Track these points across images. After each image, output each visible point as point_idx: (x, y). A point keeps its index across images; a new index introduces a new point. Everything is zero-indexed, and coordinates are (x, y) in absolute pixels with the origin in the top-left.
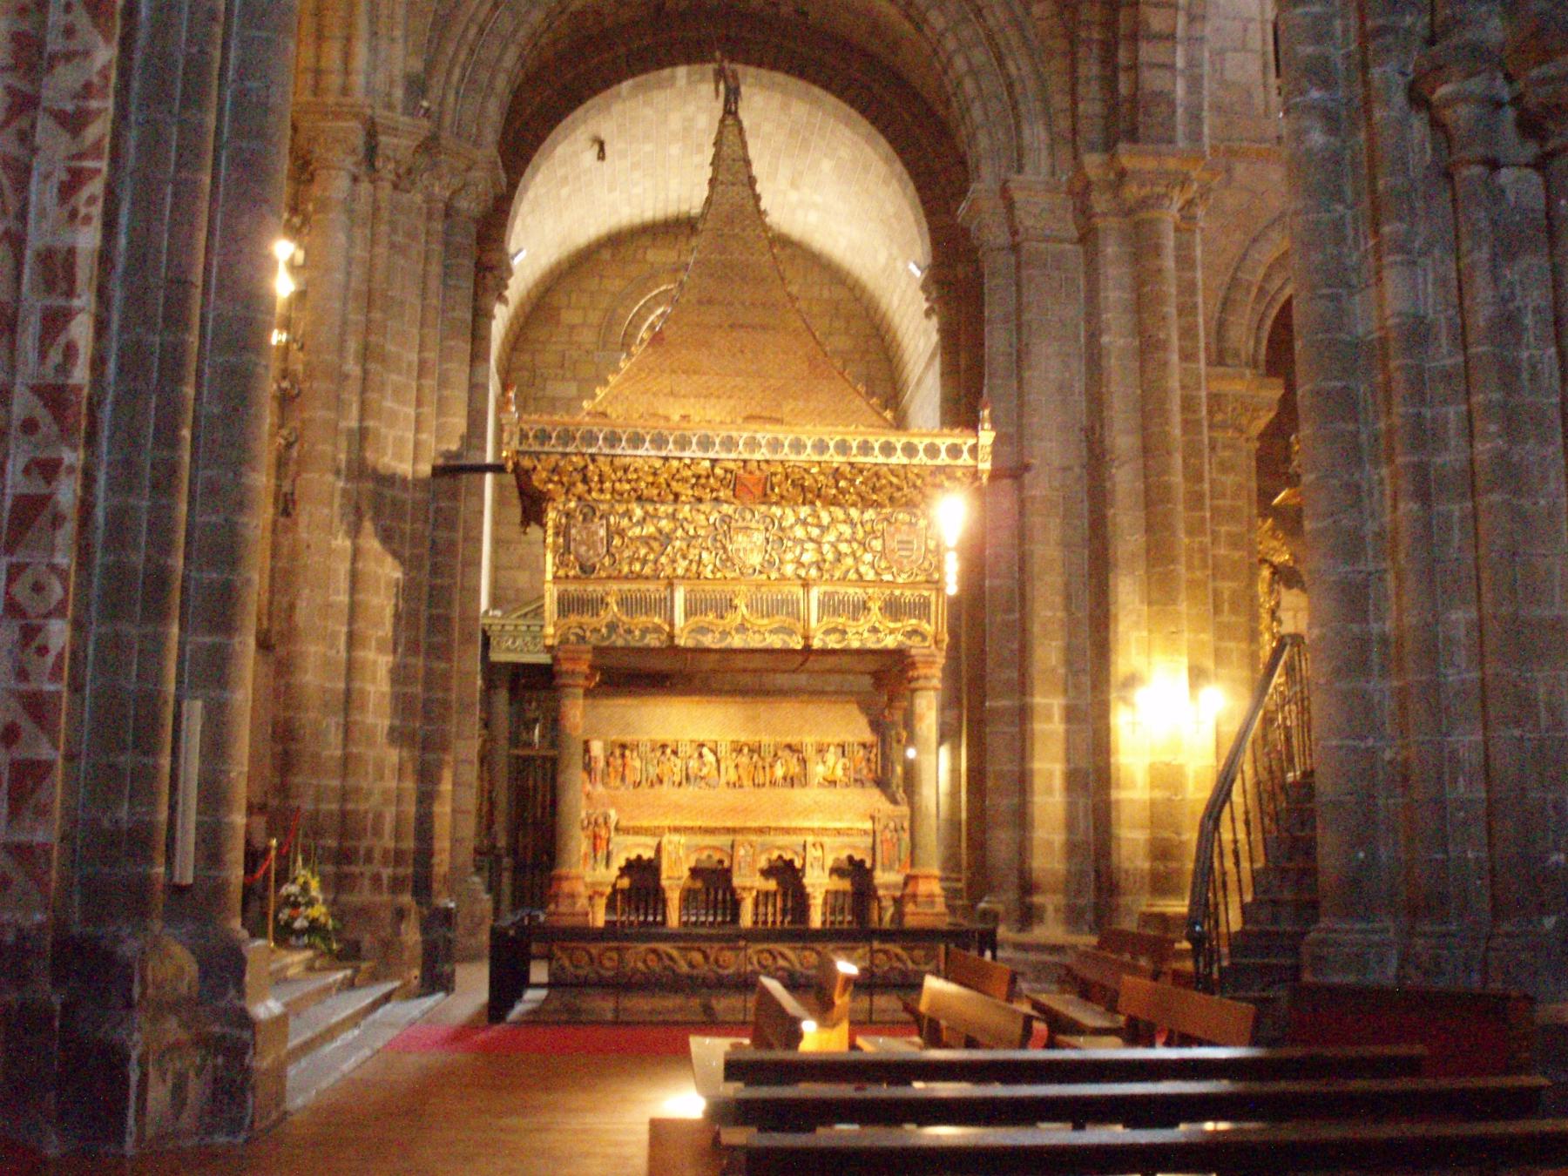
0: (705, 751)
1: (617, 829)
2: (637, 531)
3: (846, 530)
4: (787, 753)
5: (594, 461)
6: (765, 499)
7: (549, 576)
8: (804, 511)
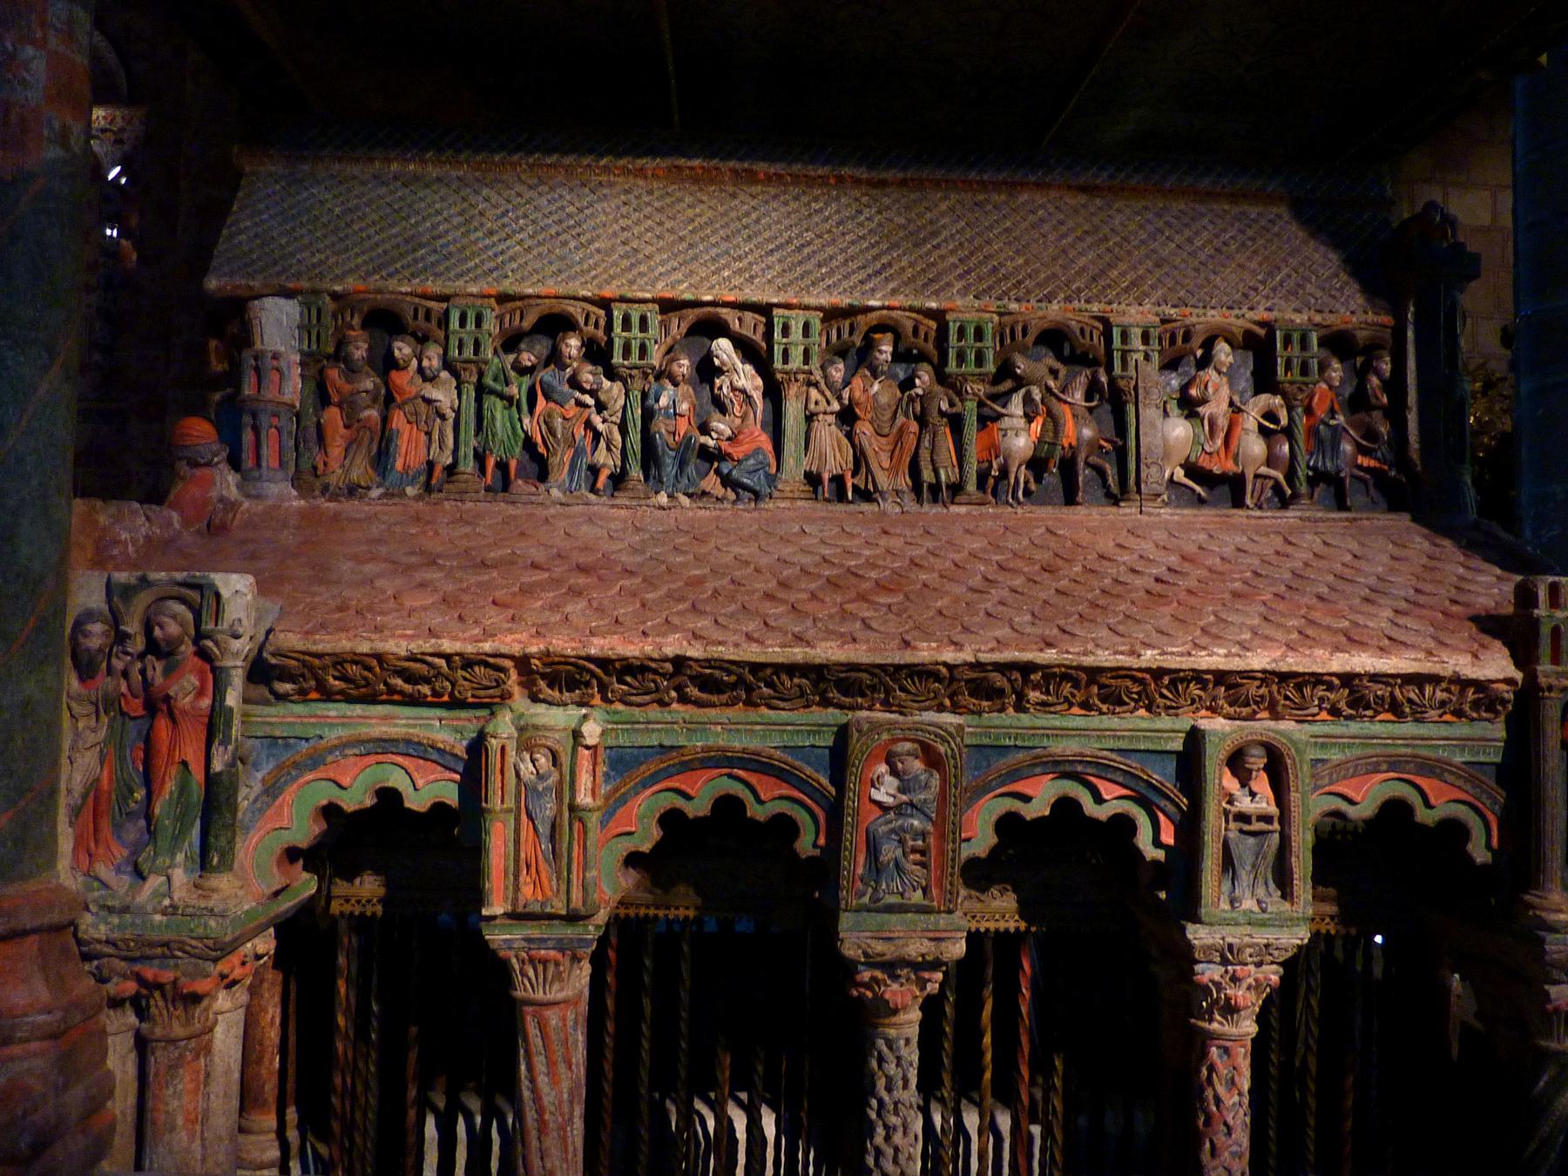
1: (261, 672)
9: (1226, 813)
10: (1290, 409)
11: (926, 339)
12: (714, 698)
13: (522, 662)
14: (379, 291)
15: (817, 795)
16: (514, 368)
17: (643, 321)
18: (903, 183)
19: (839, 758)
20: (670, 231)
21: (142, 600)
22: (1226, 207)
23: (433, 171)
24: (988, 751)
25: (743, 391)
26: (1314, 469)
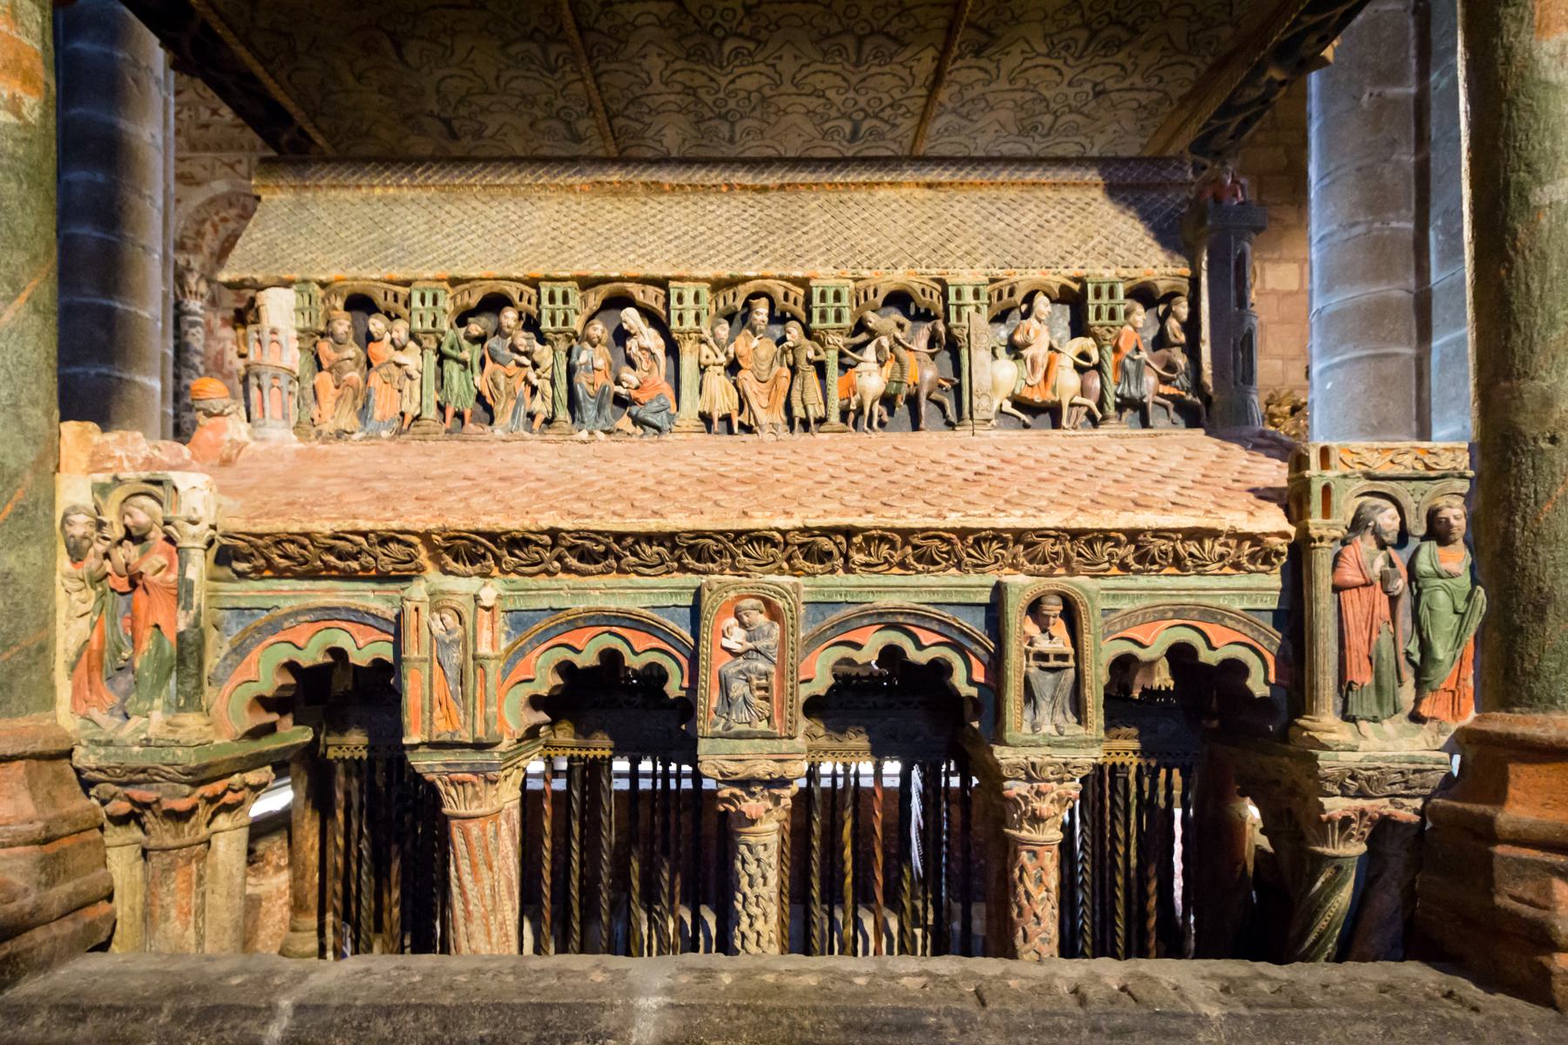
4: (886, 322)
9: (1027, 652)
10: (1100, 348)
11: (795, 303)
12: (591, 567)
13: (426, 537)
14: (355, 279)
15: (680, 646)
16: (466, 338)
17: (565, 299)
18: (782, 187)
20: (592, 230)
21: (118, 494)
22: (1050, 194)
23: (409, 194)
24: (822, 607)
25: (648, 350)
26: (1121, 396)
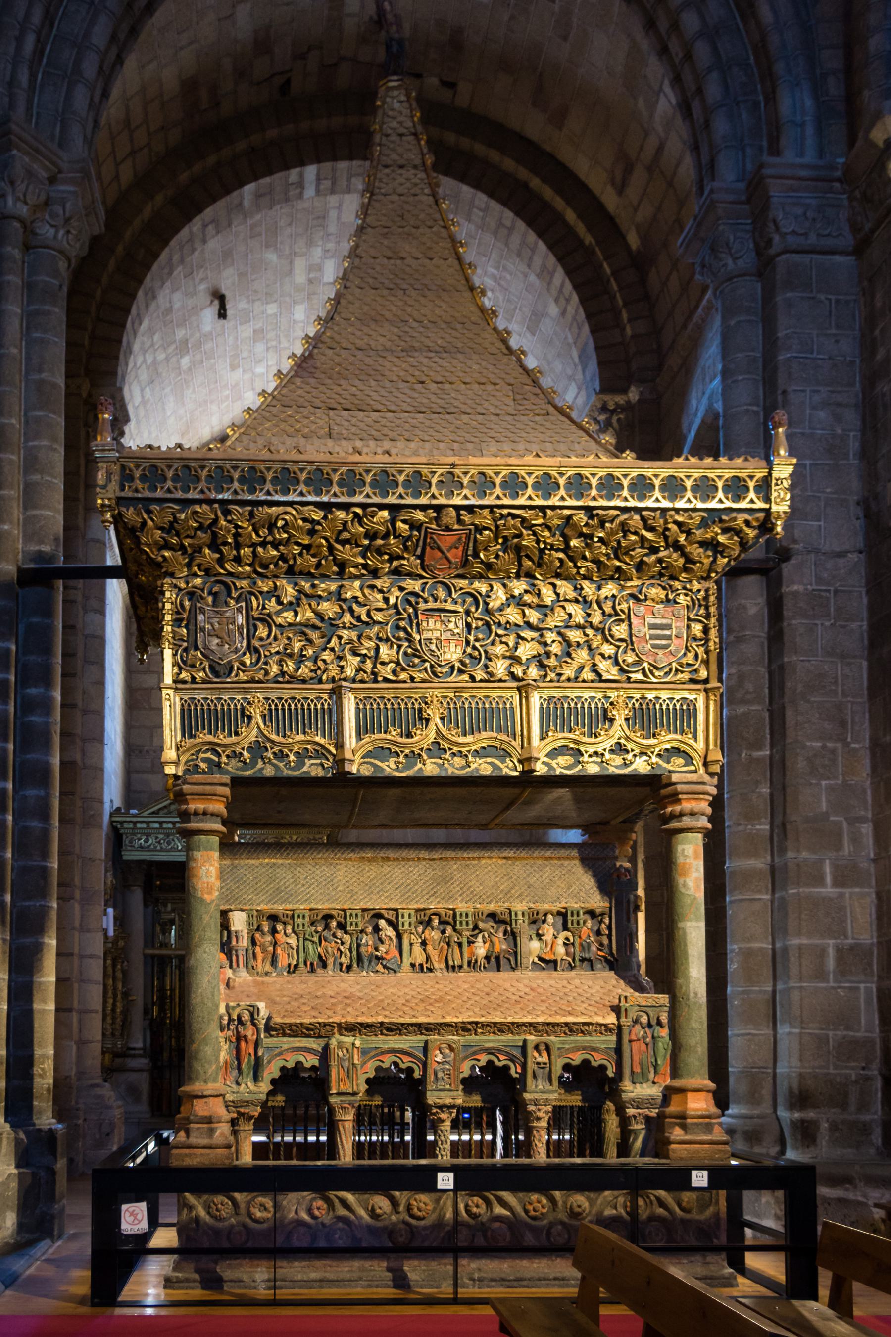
0: (382, 923)
1: (269, 1028)
2: (289, 616)
3: (577, 611)
5: (227, 513)
6: (465, 570)
7: (168, 680)
8: (519, 587)
13: (339, 1025)
19: (425, 1049)
